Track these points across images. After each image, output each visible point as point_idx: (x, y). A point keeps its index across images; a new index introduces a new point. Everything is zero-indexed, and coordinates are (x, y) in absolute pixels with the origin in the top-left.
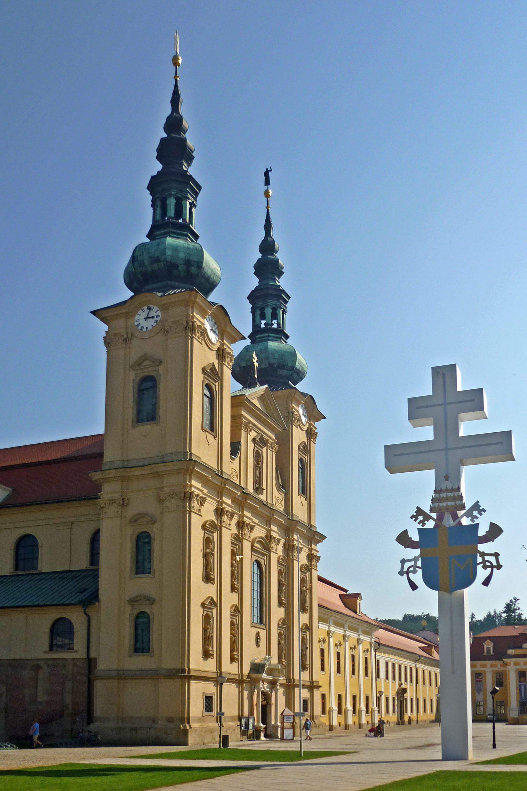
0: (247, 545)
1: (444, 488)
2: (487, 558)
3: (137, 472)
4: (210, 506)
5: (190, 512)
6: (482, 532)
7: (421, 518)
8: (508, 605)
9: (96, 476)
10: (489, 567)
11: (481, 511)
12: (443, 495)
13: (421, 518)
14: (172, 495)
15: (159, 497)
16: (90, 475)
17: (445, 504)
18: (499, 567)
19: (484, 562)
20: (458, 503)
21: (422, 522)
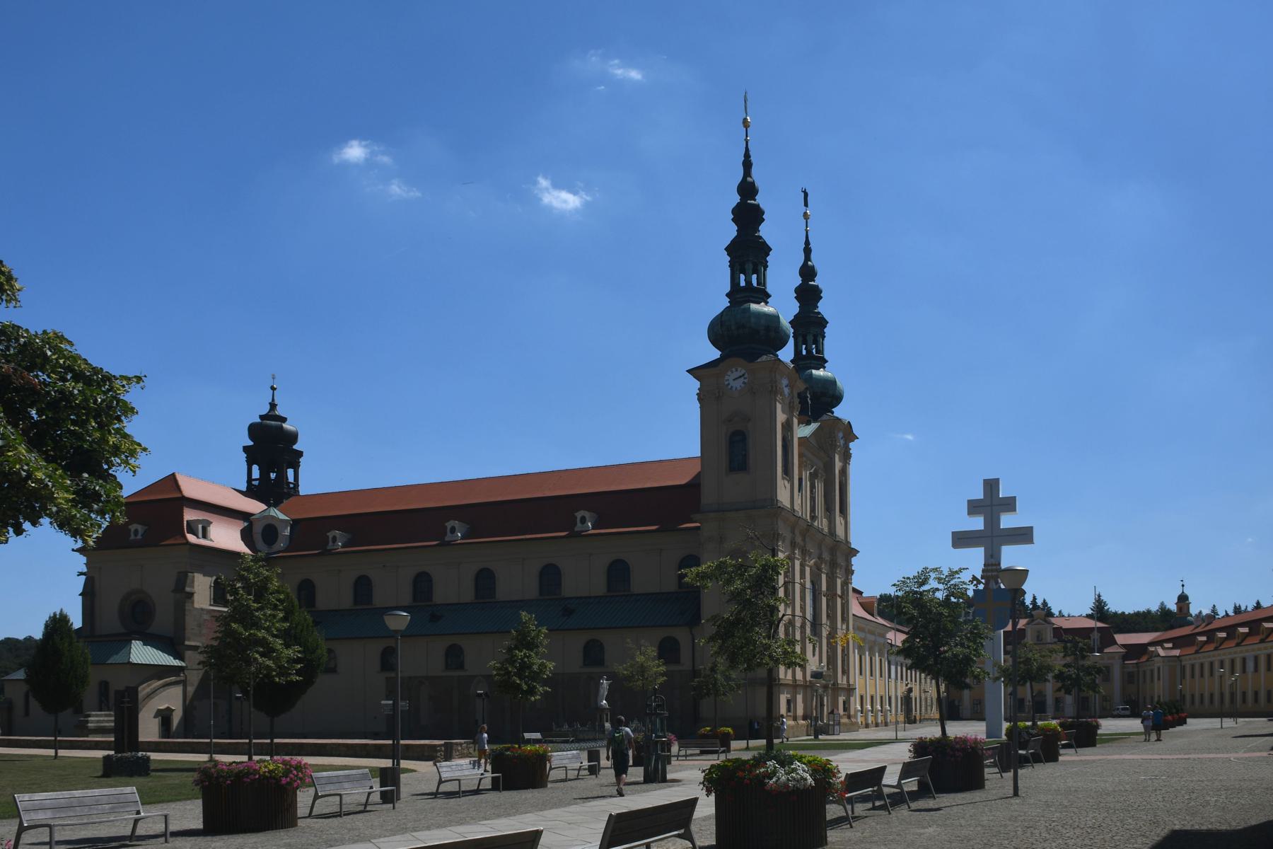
0: (808, 570)
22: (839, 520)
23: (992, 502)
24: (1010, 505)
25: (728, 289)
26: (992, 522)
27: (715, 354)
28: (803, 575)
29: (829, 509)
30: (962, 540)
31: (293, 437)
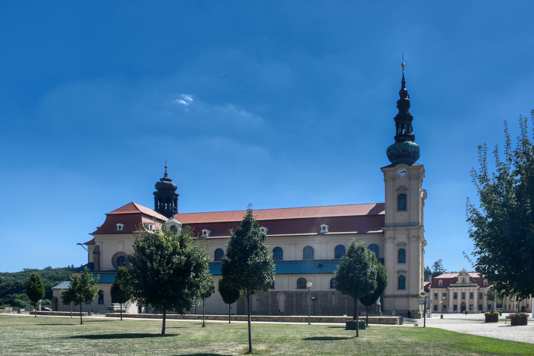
8: (436, 263)
14: (413, 237)
31: (175, 189)
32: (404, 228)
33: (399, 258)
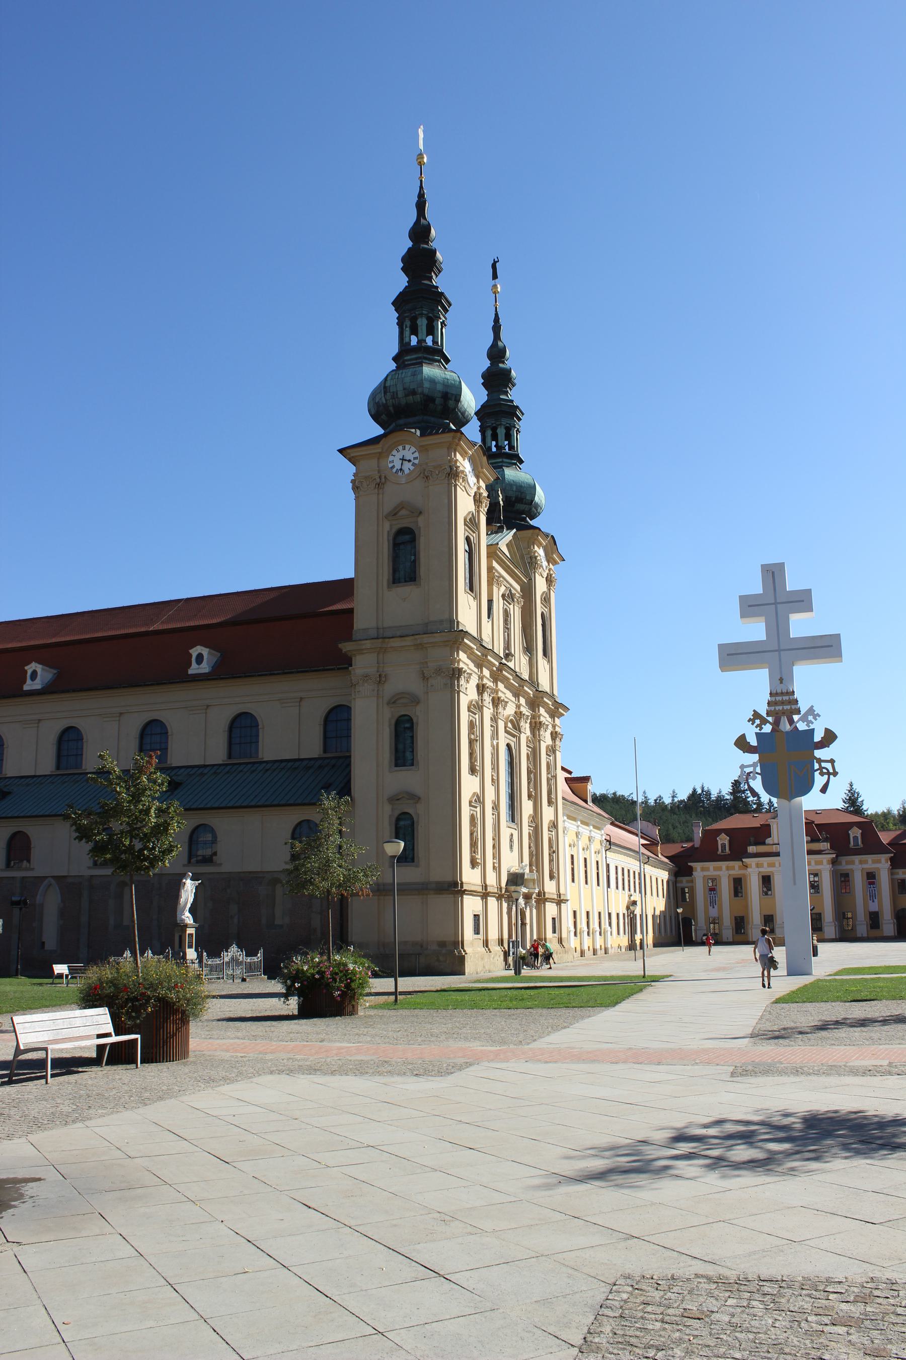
0: (501, 724)
1: (779, 691)
2: (823, 765)
3: (396, 643)
4: (474, 681)
5: (458, 693)
6: (818, 737)
7: (758, 722)
9: (346, 647)
10: (825, 773)
11: (816, 716)
12: (779, 698)
13: (758, 722)
15: (423, 674)
16: (340, 646)
17: (780, 708)
18: (835, 774)
19: (821, 768)
20: (793, 707)
21: (760, 726)
22: (542, 662)
23: (775, 598)
24: (802, 601)
25: (395, 350)
26: (778, 627)
27: (380, 431)
28: (495, 735)
29: (529, 649)
30: (734, 656)
32: (408, 641)
33: (396, 750)
